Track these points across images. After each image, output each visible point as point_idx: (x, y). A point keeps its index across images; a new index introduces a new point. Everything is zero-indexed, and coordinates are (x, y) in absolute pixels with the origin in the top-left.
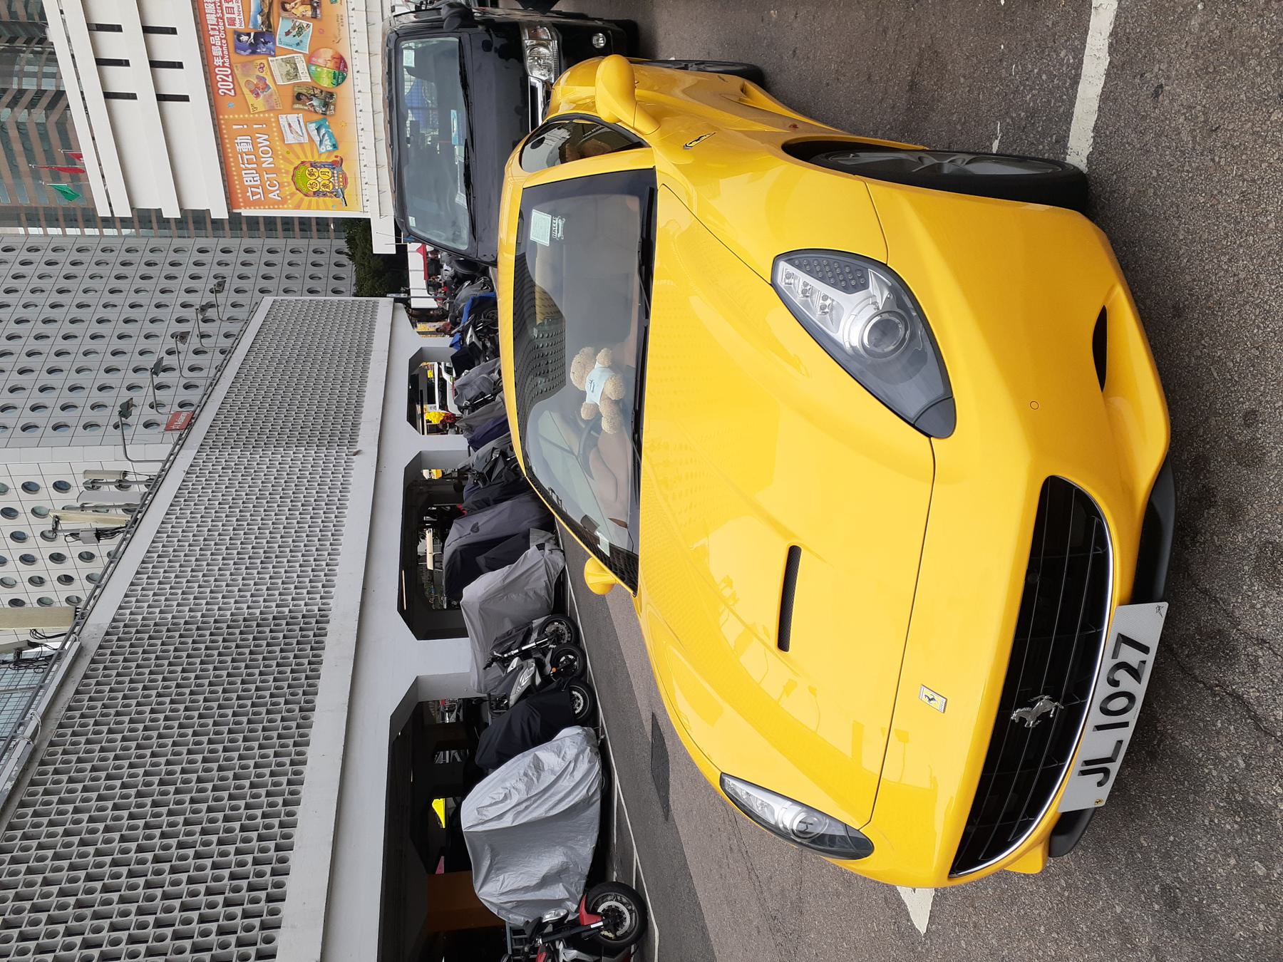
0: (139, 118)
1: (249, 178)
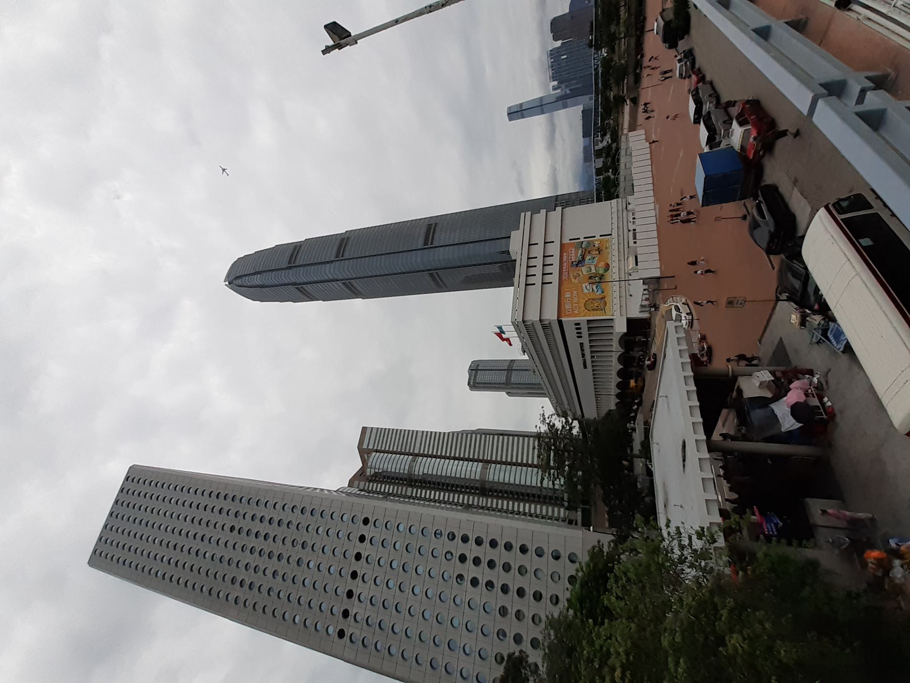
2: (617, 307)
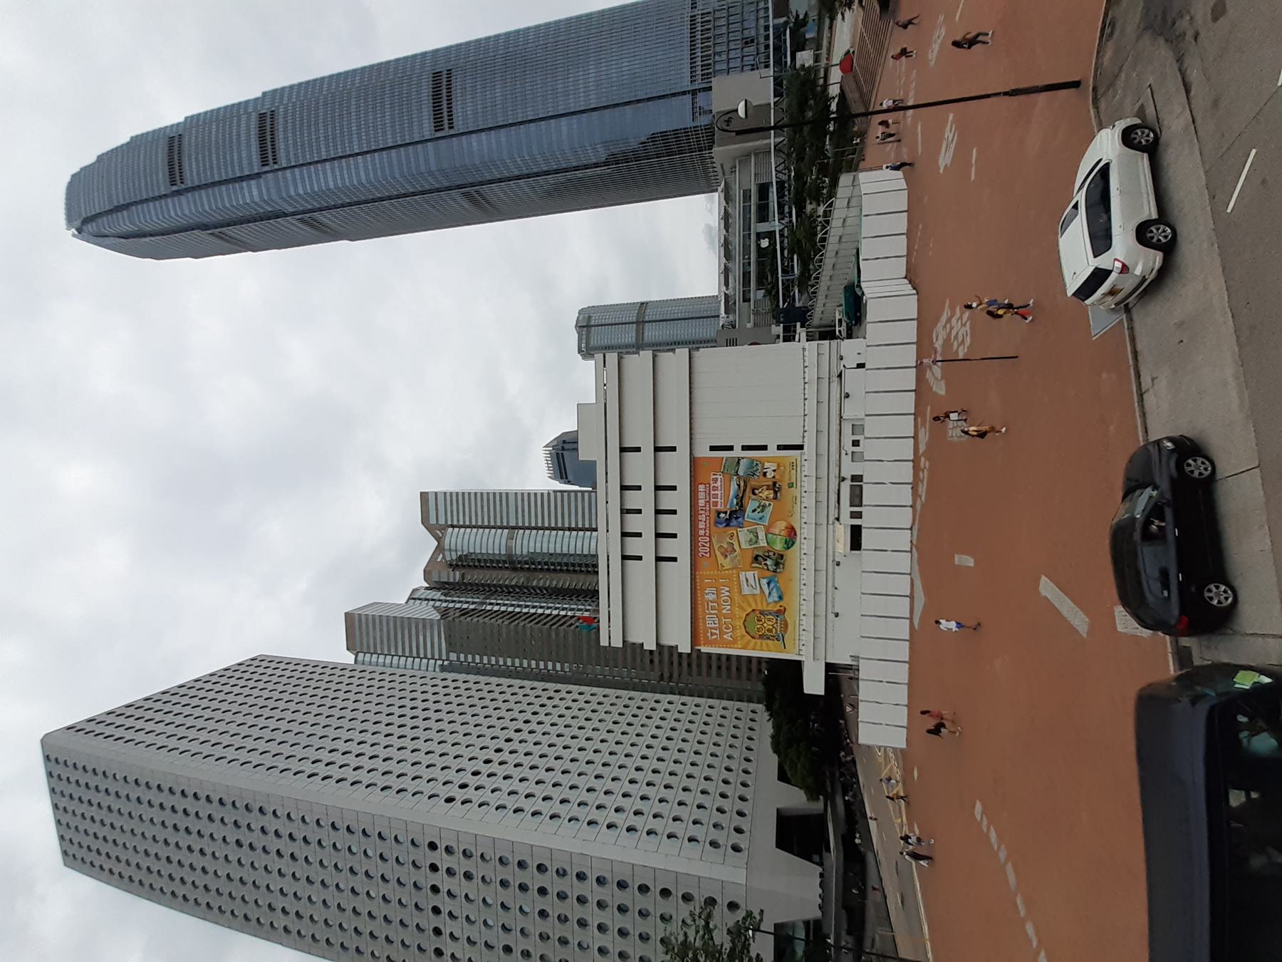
0: (642, 573)
1: (710, 622)
2: (807, 638)
